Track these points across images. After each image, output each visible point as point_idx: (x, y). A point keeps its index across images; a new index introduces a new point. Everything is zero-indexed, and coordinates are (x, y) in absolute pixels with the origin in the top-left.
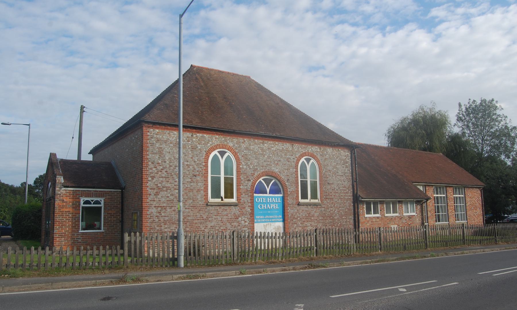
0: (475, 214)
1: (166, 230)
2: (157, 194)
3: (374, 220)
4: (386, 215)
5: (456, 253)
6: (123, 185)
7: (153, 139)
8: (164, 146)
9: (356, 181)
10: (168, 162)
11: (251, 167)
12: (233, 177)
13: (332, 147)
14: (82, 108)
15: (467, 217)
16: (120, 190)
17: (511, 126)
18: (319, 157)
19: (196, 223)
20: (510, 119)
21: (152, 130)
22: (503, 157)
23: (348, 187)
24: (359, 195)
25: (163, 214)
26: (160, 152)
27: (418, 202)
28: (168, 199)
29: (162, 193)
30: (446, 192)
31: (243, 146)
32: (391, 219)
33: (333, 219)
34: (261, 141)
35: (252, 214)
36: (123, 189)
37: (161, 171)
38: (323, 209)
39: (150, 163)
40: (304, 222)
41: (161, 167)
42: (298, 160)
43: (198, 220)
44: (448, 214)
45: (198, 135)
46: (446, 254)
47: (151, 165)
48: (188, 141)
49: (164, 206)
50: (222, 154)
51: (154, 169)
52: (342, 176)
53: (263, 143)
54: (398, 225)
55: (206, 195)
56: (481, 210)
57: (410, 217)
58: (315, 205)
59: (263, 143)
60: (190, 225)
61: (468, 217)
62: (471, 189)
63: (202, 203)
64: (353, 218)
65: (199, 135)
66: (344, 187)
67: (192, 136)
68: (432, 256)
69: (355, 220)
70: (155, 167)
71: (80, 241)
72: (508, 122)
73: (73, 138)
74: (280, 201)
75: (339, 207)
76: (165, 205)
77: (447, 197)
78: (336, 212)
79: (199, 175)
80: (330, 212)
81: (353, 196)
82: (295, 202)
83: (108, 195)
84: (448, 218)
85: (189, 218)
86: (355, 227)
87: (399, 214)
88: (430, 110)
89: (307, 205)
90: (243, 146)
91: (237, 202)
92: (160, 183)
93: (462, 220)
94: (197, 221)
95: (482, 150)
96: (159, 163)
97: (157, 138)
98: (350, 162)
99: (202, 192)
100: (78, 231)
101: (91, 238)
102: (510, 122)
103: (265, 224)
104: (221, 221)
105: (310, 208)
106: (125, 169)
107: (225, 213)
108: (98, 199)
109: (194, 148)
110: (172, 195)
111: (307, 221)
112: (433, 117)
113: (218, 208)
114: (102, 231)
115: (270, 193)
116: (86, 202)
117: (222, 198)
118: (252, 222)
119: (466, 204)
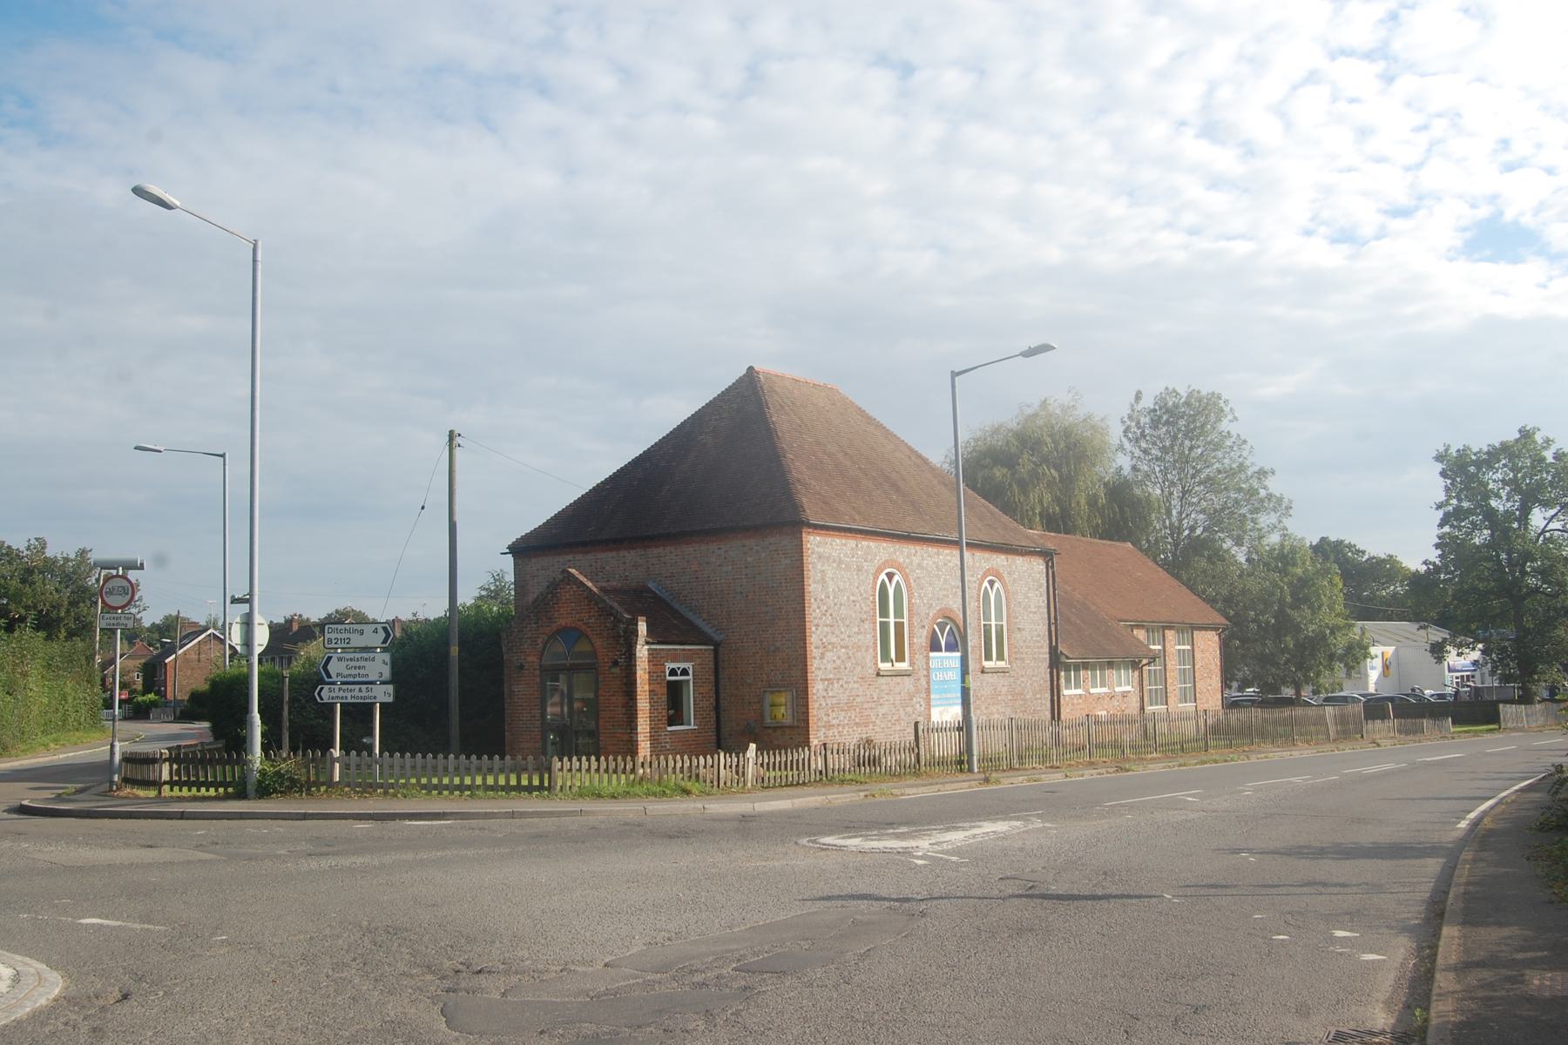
0: (1209, 688)
1: (834, 722)
2: (822, 658)
3: (1075, 701)
4: (1093, 691)
5: (1259, 756)
6: (717, 637)
7: (814, 556)
8: (826, 567)
9: (1056, 623)
10: (831, 597)
11: (925, 602)
12: (903, 623)
13: (1023, 556)
14: (452, 436)
15: (1195, 695)
16: (712, 647)
17: (1253, 464)
18: (1005, 575)
19: (866, 709)
20: (1252, 447)
21: (812, 538)
22: (1228, 544)
23: (1044, 636)
24: (1061, 652)
25: (830, 694)
26: (823, 580)
27: (1135, 665)
28: (835, 665)
29: (829, 654)
30: (1164, 640)
31: (916, 560)
32: (1099, 698)
33: (1025, 700)
34: (935, 550)
35: (928, 691)
36: (717, 645)
37: (825, 615)
38: (1012, 680)
39: (813, 600)
40: (989, 704)
41: (825, 608)
42: (981, 585)
43: (868, 702)
44: (1166, 688)
45: (863, 543)
46: (1248, 757)
47: (814, 606)
48: (853, 557)
49: (830, 679)
50: (890, 576)
51: (818, 611)
52: (1035, 613)
53: (938, 554)
54: (1108, 712)
55: (876, 657)
56: (1219, 679)
57: (1124, 695)
58: (1003, 671)
59: (938, 554)
60: (860, 713)
61: (1197, 695)
62: (1203, 632)
63: (872, 671)
64: (1049, 698)
65: (865, 543)
66: (1039, 636)
67: (857, 546)
68: (1232, 760)
69: (1052, 701)
70: (819, 608)
71: (668, 747)
72: (1245, 454)
73: (423, 508)
74: (958, 664)
75: (1033, 676)
76: (831, 676)
77: (1164, 651)
78: (1028, 684)
79: (867, 620)
80: (1020, 685)
81: (1050, 653)
82: (978, 666)
83: (699, 658)
84: (1166, 697)
85: (858, 700)
86: (1053, 718)
87: (1109, 689)
88: (1064, 409)
89: (996, 671)
90: (916, 560)
91: (911, 668)
92: (825, 637)
93: (1157, 704)
94: (865, 706)
95: (1180, 521)
96: (822, 600)
97: (818, 553)
98: (1045, 584)
99: (871, 650)
100: (665, 728)
101: (682, 741)
102: (1250, 452)
103: (941, 708)
104: (894, 704)
105: (996, 678)
106: (721, 605)
107: (897, 690)
108: (682, 665)
109: (859, 569)
110: (839, 658)
111: (993, 704)
112: (1067, 433)
113: (890, 678)
114: (692, 727)
115: (946, 651)
116: (673, 672)
117: (892, 661)
118: (929, 707)
119: (1194, 667)
